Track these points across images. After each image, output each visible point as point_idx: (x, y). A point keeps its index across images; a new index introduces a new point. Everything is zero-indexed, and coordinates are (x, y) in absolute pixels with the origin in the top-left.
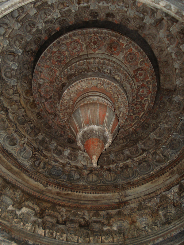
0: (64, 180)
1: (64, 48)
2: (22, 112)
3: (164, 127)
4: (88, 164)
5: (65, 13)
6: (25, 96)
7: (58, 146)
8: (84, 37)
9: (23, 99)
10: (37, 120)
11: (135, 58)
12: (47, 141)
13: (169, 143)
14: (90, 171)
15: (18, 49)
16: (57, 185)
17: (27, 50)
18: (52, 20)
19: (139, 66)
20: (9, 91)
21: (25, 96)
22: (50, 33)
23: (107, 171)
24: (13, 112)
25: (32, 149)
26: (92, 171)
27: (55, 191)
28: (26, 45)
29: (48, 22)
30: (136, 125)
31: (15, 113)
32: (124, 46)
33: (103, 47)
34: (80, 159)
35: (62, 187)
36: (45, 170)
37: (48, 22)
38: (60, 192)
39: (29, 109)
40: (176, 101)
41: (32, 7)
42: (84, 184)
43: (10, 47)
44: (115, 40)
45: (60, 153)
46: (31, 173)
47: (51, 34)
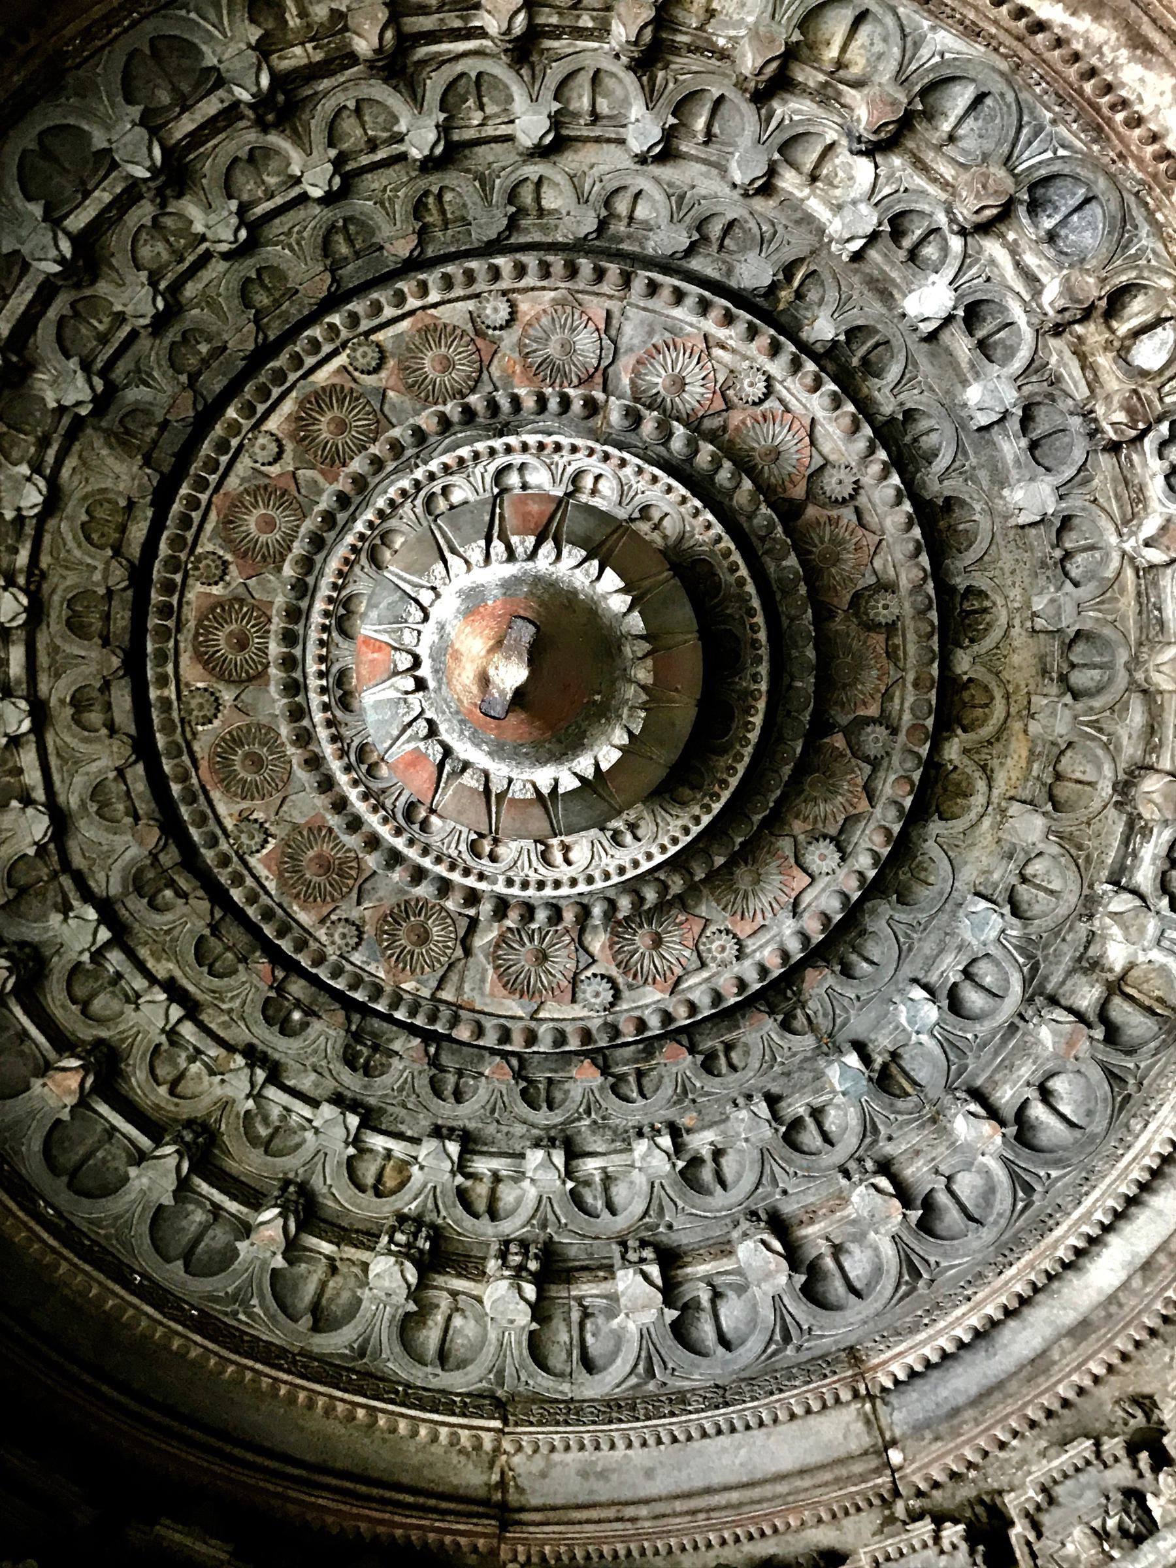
0: (1054, 122)
1: (595, 993)
2: (1044, 722)
3: (213, 218)
4: (831, 147)
5: (507, 1133)
6: (981, 785)
7: (965, 366)
8: (459, 989)
9: (1000, 779)
10: (1000, 601)
11: (235, 754)
12: (1017, 437)
13: (210, 92)
14: (839, 93)
15: (844, 1094)
16: (1109, 121)
17: (805, 1043)
18: (594, 1132)
19: (227, 696)
20: (1048, 872)
21: (981, 785)
22: (646, 1060)
23: (721, 42)
24: (1106, 746)
25: (1135, 457)
26: (826, 85)
27: (1150, 76)
28: (801, 1069)
29: (620, 1130)
30: (389, 312)
31: (1094, 738)
32: (270, 847)
33: (381, 893)
34: (864, 208)
35: (1080, 92)
36: (1133, 274)
37: (620, 1130)
38: (1124, 53)
39: (1007, 696)
40: (79, 373)
41: (627, 1315)
42: (926, 24)
43: (881, 1127)
44: (302, 908)
45: (973, 314)
46: (1035, 773)
47: (639, 1052)
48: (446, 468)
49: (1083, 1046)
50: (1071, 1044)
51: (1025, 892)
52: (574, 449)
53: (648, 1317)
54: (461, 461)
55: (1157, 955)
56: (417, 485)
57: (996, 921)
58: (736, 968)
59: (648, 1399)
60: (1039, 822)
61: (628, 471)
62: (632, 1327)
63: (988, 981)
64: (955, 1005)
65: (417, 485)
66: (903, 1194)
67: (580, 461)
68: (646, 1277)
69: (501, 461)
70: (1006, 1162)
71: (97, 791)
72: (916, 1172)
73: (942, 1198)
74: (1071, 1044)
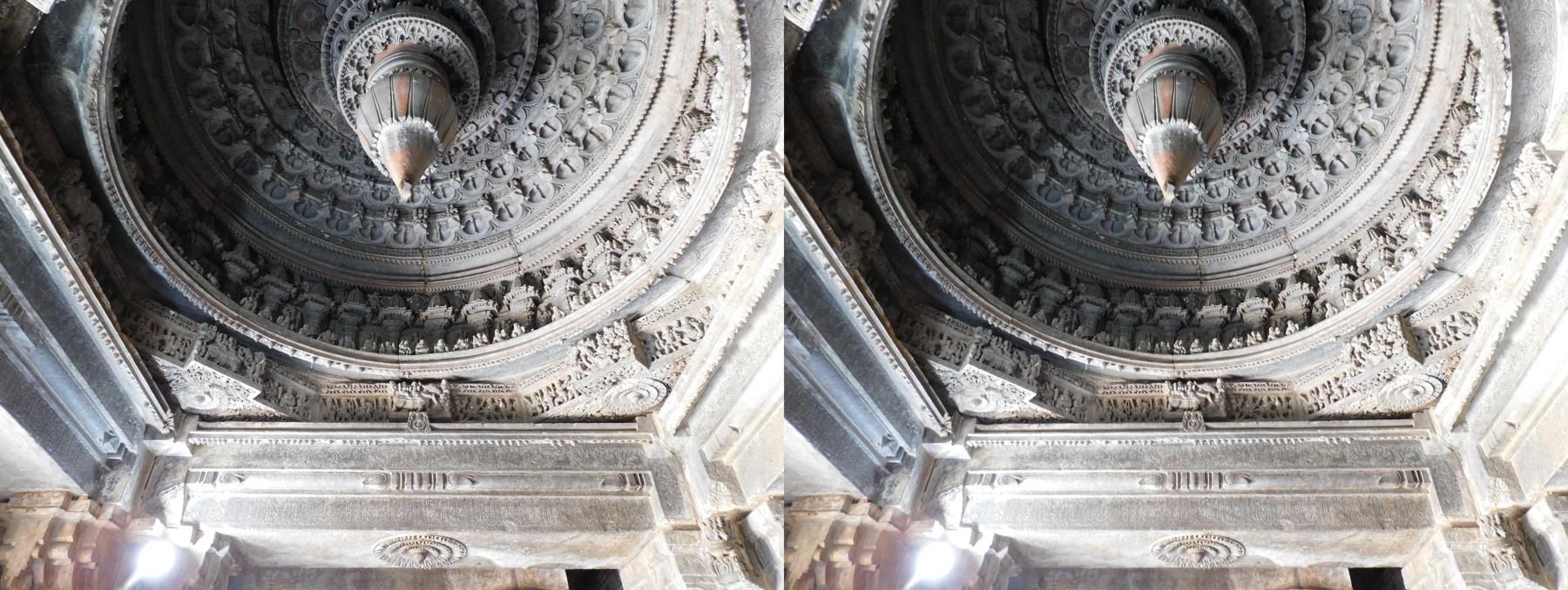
48: (370, 34)
49: (577, 153)
50: (573, 152)
51: (565, 97)
52: (411, 21)
53: (457, 229)
54: (374, 31)
55: (601, 125)
56: (362, 40)
57: (555, 111)
58: (476, 134)
59: (459, 246)
60: (570, 79)
61: (430, 26)
62: (453, 231)
63: (552, 125)
64: (542, 134)
65: (362, 40)
66: (524, 189)
67: (413, 24)
68: (455, 219)
69: (387, 28)
70: (553, 184)
71: (278, 102)
72: (529, 184)
73: (536, 190)
74: (573, 152)
